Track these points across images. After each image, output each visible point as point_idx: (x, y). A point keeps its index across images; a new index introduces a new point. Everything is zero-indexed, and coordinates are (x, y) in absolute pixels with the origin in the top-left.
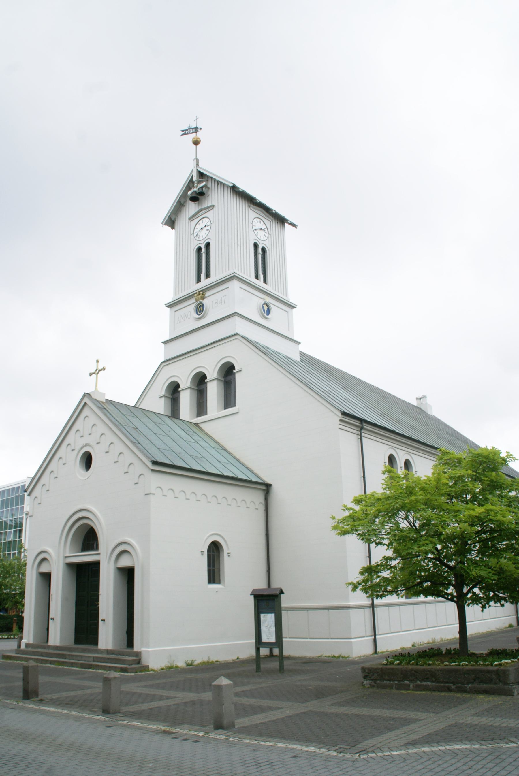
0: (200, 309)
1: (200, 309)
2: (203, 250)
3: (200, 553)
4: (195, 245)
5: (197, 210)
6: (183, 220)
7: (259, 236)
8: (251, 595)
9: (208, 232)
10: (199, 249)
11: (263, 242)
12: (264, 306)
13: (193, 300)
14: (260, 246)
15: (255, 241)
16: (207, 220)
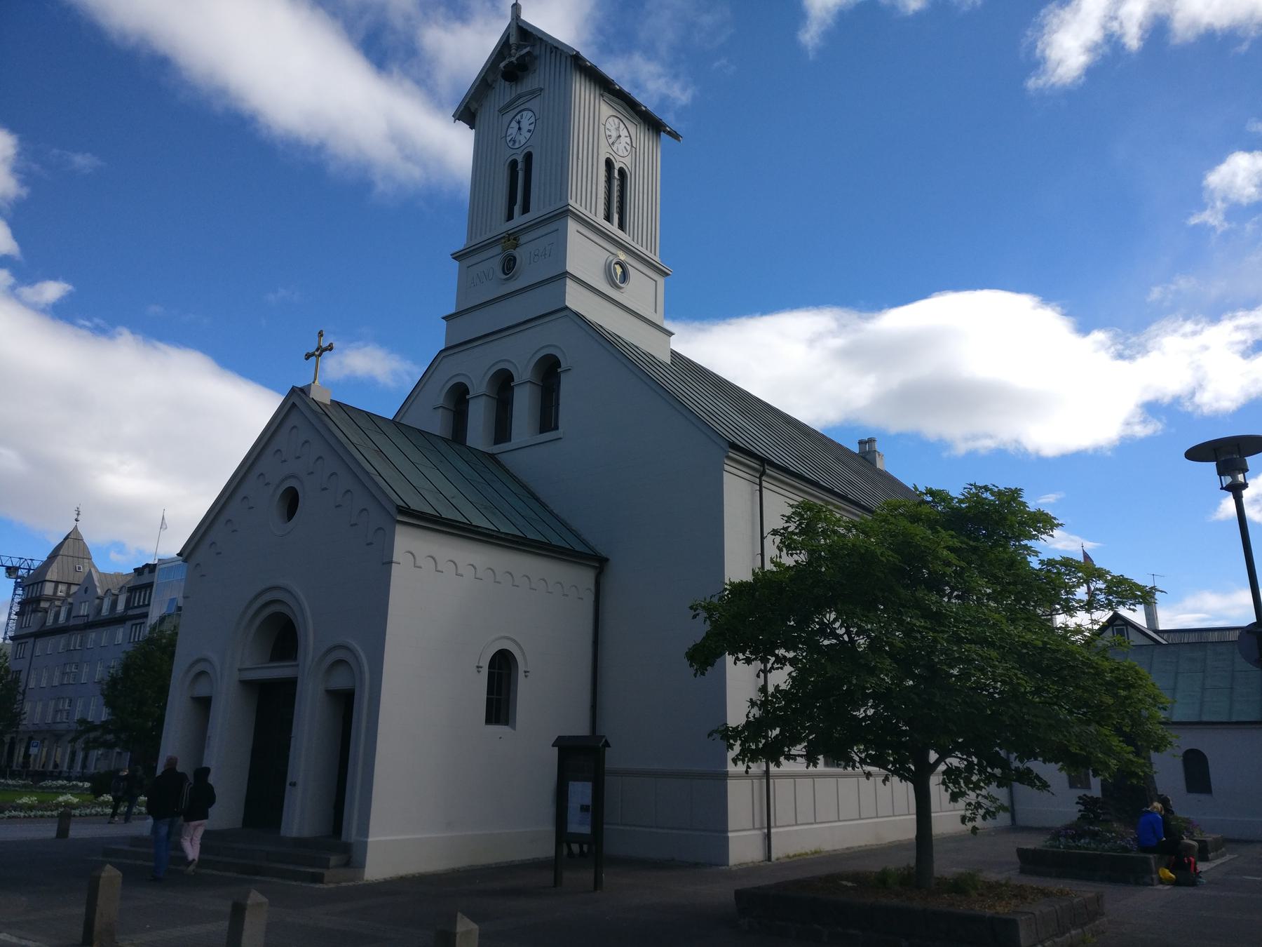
0: (509, 265)
1: (509, 265)
2: (520, 166)
3: (476, 670)
4: (506, 156)
5: (513, 96)
6: (488, 113)
8: (553, 746)
9: (530, 134)
10: (514, 164)
11: (622, 159)
12: (616, 266)
13: (497, 250)
14: (617, 166)
15: (608, 156)
16: (530, 114)
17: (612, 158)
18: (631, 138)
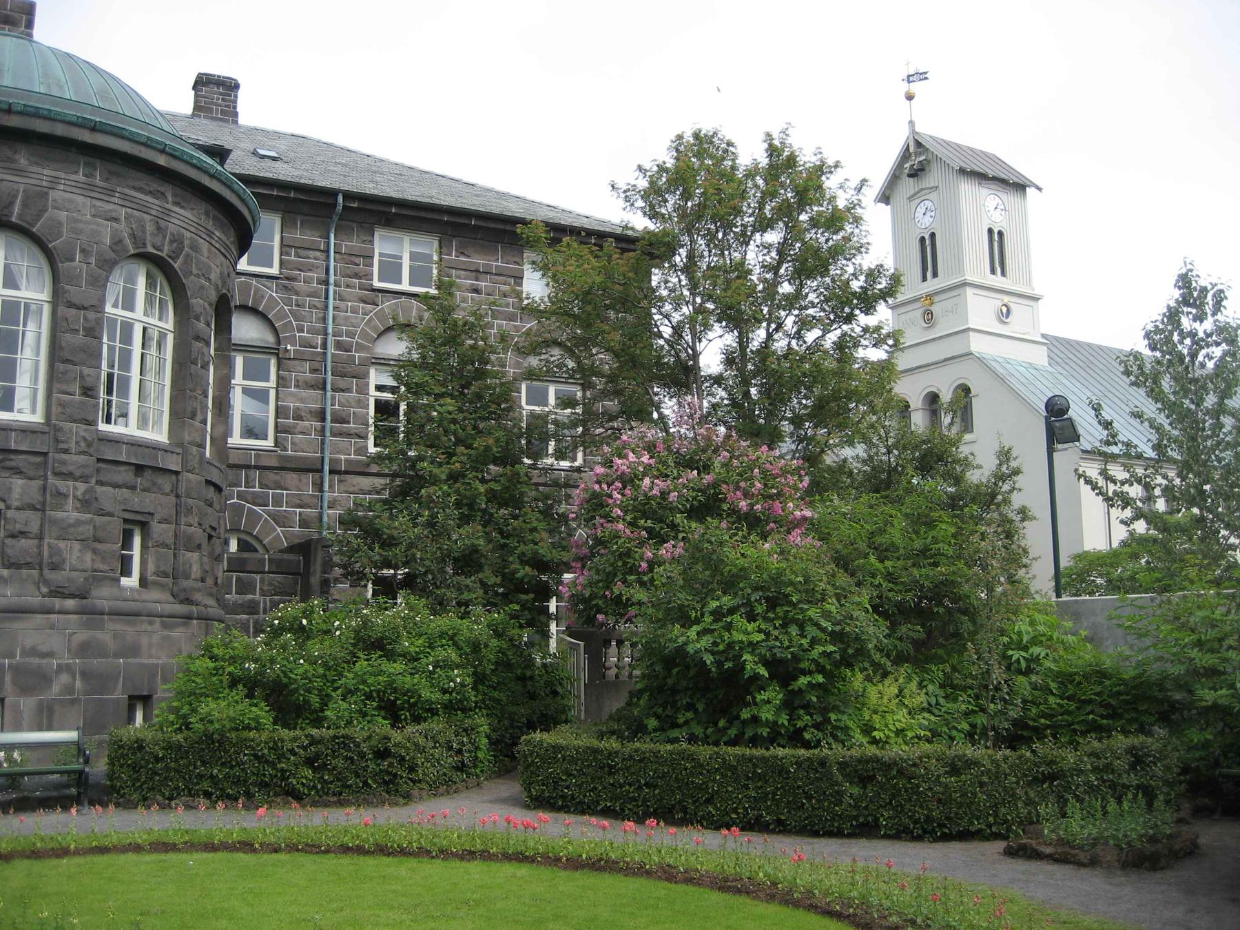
0: (929, 317)
2: (928, 242)
10: (923, 239)
14: (996, 231)
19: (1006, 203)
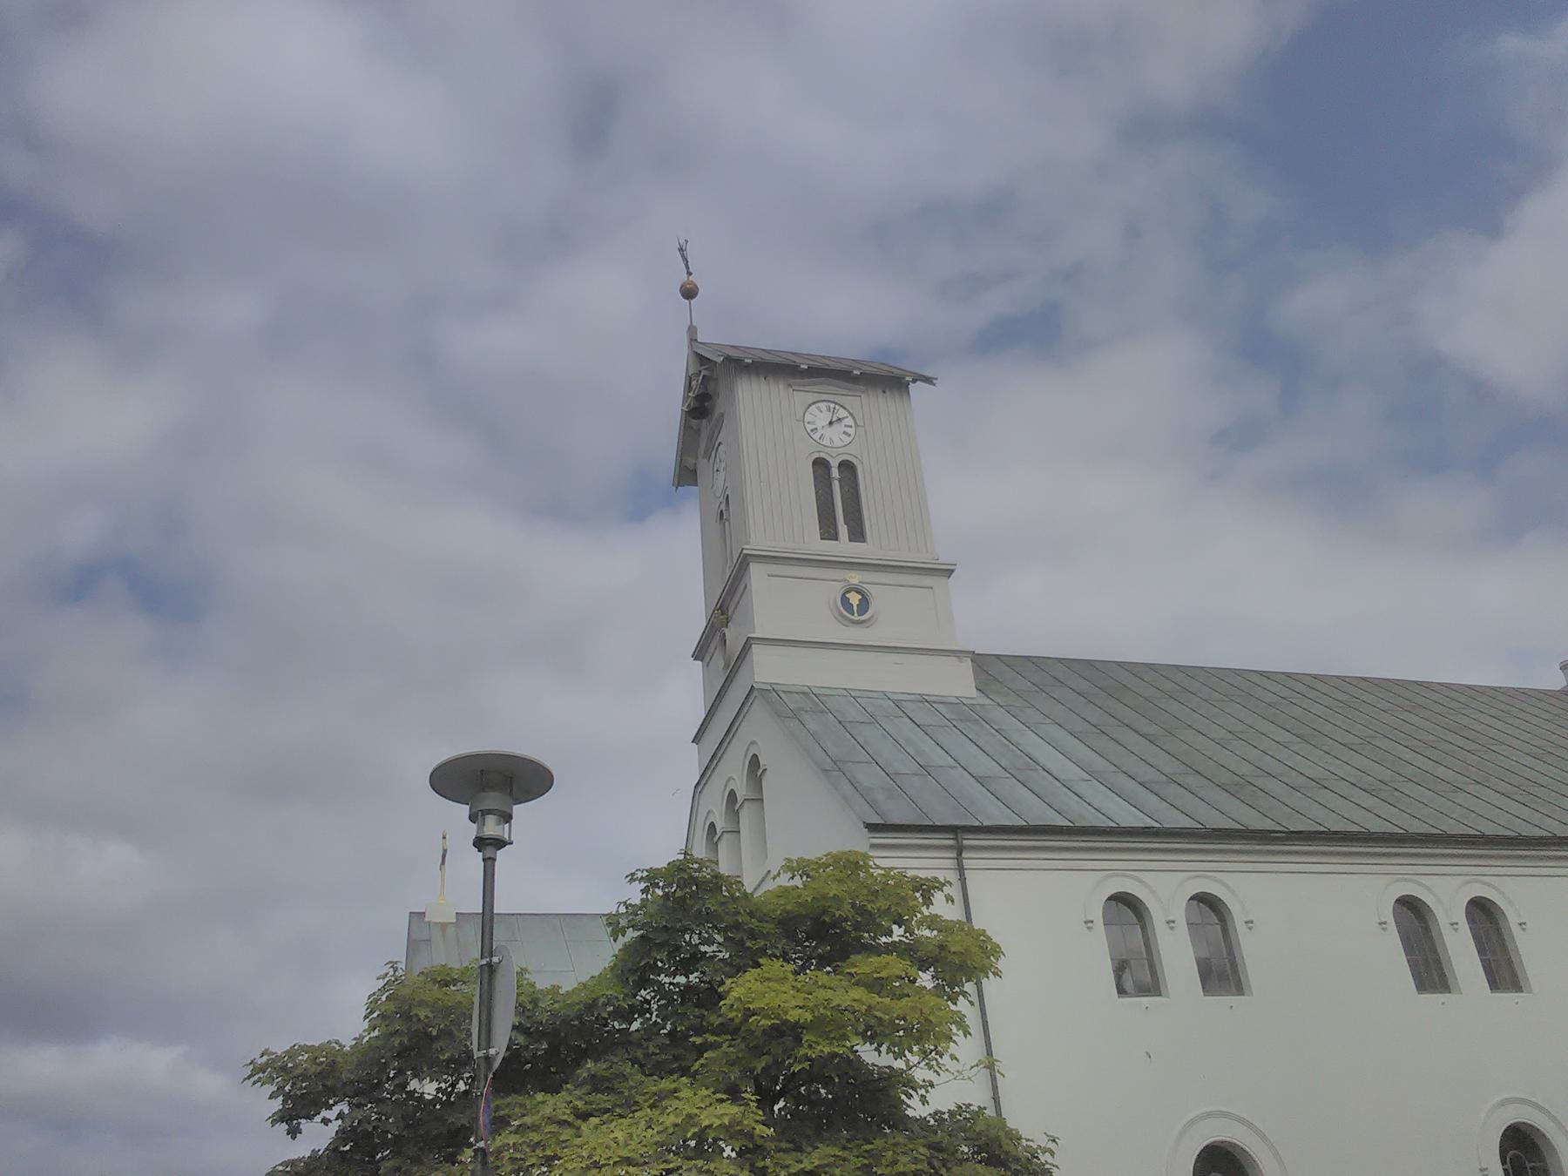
7: (826, 442)
11: (841, 450)
12: (847, 595)
14: (834, 463)
15: (816, 455)
17: (823, 455)
18: (854, 418)
19: (858, 416)
